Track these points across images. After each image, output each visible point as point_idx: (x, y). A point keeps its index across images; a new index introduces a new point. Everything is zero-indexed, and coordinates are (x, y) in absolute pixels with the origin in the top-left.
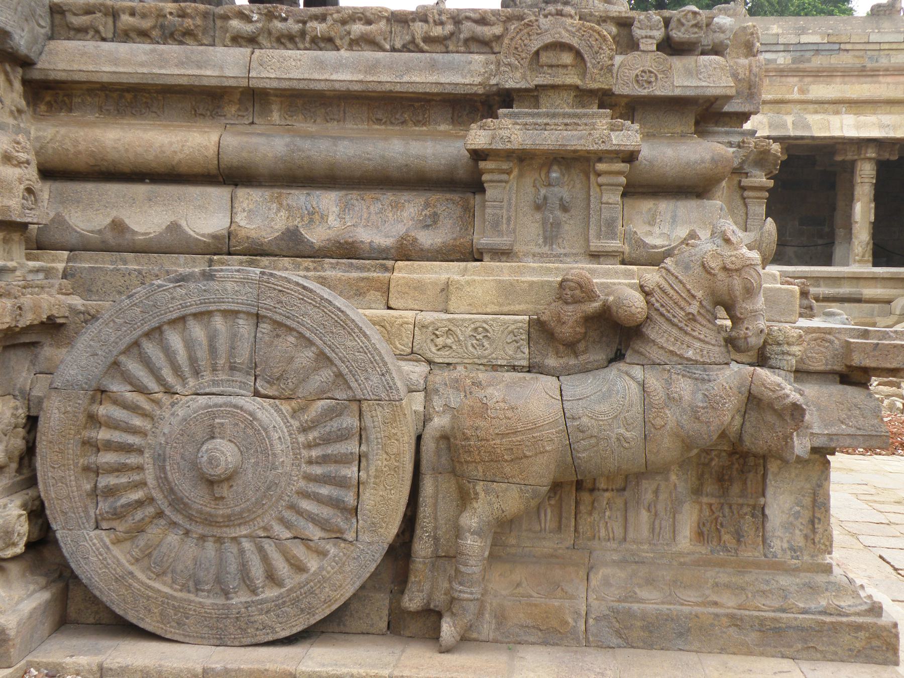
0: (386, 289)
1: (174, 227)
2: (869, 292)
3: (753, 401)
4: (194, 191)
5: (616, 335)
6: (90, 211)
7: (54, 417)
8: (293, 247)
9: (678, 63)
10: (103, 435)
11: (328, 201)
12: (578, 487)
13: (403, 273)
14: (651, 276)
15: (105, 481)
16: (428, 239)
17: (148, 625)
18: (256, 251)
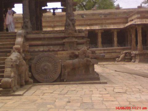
0: (57, 54)
1: (39, 50)
2: (117, 51)
3: (87, 61)
4: (40, 47)
5: (76, 56)
6: (32, 49)
7: (33, 65)
8: (49, 51)
9: (80, 33)
10: (36, 67)
11: (51, 47)
12: (74, 69)
13: (59, 52)
14: (79, 51)
15: (37, 71)
16: (60, 49)
17: (41, 82)
18: (46, 51)
